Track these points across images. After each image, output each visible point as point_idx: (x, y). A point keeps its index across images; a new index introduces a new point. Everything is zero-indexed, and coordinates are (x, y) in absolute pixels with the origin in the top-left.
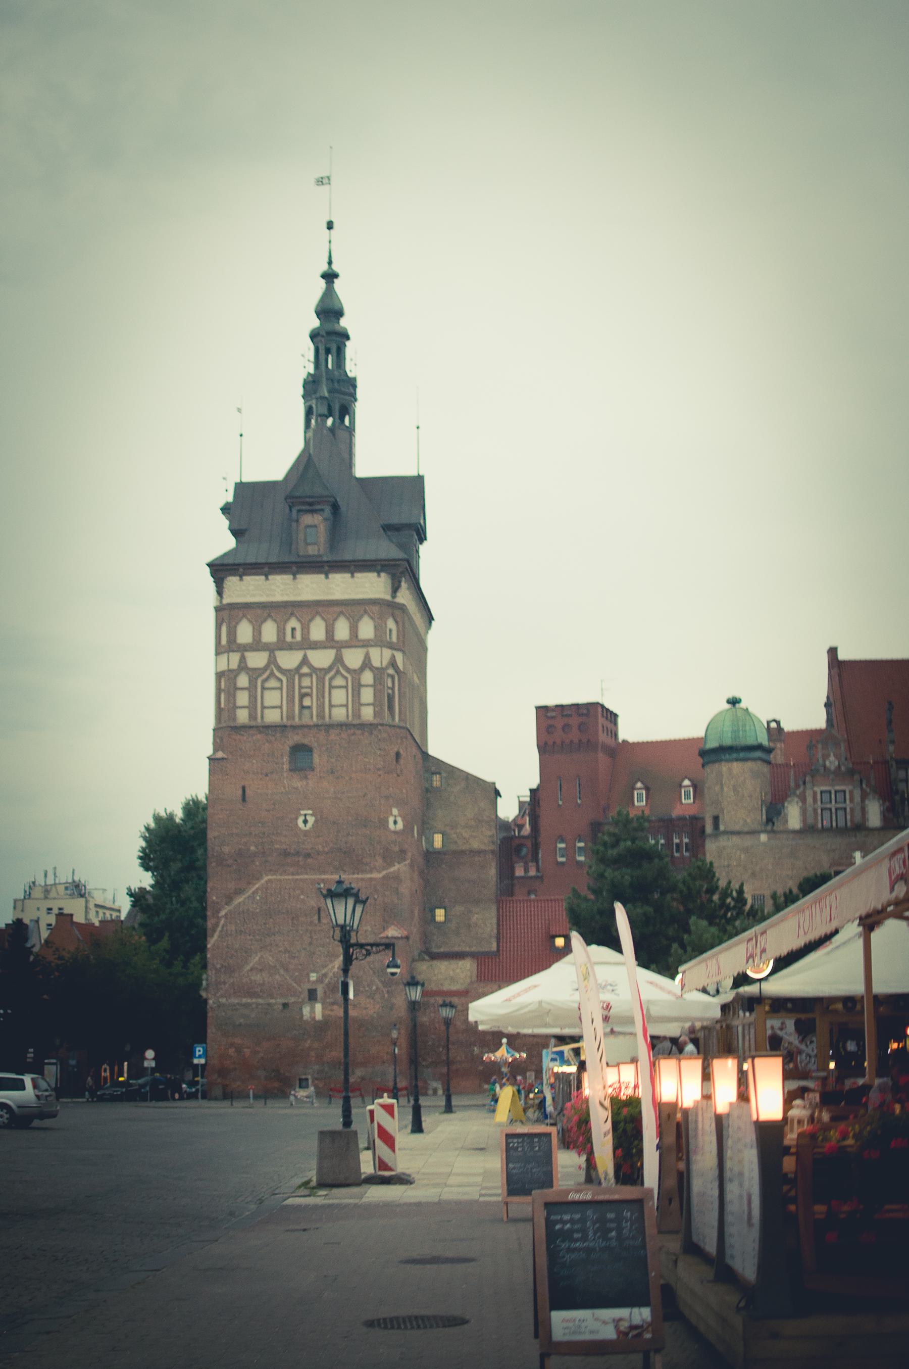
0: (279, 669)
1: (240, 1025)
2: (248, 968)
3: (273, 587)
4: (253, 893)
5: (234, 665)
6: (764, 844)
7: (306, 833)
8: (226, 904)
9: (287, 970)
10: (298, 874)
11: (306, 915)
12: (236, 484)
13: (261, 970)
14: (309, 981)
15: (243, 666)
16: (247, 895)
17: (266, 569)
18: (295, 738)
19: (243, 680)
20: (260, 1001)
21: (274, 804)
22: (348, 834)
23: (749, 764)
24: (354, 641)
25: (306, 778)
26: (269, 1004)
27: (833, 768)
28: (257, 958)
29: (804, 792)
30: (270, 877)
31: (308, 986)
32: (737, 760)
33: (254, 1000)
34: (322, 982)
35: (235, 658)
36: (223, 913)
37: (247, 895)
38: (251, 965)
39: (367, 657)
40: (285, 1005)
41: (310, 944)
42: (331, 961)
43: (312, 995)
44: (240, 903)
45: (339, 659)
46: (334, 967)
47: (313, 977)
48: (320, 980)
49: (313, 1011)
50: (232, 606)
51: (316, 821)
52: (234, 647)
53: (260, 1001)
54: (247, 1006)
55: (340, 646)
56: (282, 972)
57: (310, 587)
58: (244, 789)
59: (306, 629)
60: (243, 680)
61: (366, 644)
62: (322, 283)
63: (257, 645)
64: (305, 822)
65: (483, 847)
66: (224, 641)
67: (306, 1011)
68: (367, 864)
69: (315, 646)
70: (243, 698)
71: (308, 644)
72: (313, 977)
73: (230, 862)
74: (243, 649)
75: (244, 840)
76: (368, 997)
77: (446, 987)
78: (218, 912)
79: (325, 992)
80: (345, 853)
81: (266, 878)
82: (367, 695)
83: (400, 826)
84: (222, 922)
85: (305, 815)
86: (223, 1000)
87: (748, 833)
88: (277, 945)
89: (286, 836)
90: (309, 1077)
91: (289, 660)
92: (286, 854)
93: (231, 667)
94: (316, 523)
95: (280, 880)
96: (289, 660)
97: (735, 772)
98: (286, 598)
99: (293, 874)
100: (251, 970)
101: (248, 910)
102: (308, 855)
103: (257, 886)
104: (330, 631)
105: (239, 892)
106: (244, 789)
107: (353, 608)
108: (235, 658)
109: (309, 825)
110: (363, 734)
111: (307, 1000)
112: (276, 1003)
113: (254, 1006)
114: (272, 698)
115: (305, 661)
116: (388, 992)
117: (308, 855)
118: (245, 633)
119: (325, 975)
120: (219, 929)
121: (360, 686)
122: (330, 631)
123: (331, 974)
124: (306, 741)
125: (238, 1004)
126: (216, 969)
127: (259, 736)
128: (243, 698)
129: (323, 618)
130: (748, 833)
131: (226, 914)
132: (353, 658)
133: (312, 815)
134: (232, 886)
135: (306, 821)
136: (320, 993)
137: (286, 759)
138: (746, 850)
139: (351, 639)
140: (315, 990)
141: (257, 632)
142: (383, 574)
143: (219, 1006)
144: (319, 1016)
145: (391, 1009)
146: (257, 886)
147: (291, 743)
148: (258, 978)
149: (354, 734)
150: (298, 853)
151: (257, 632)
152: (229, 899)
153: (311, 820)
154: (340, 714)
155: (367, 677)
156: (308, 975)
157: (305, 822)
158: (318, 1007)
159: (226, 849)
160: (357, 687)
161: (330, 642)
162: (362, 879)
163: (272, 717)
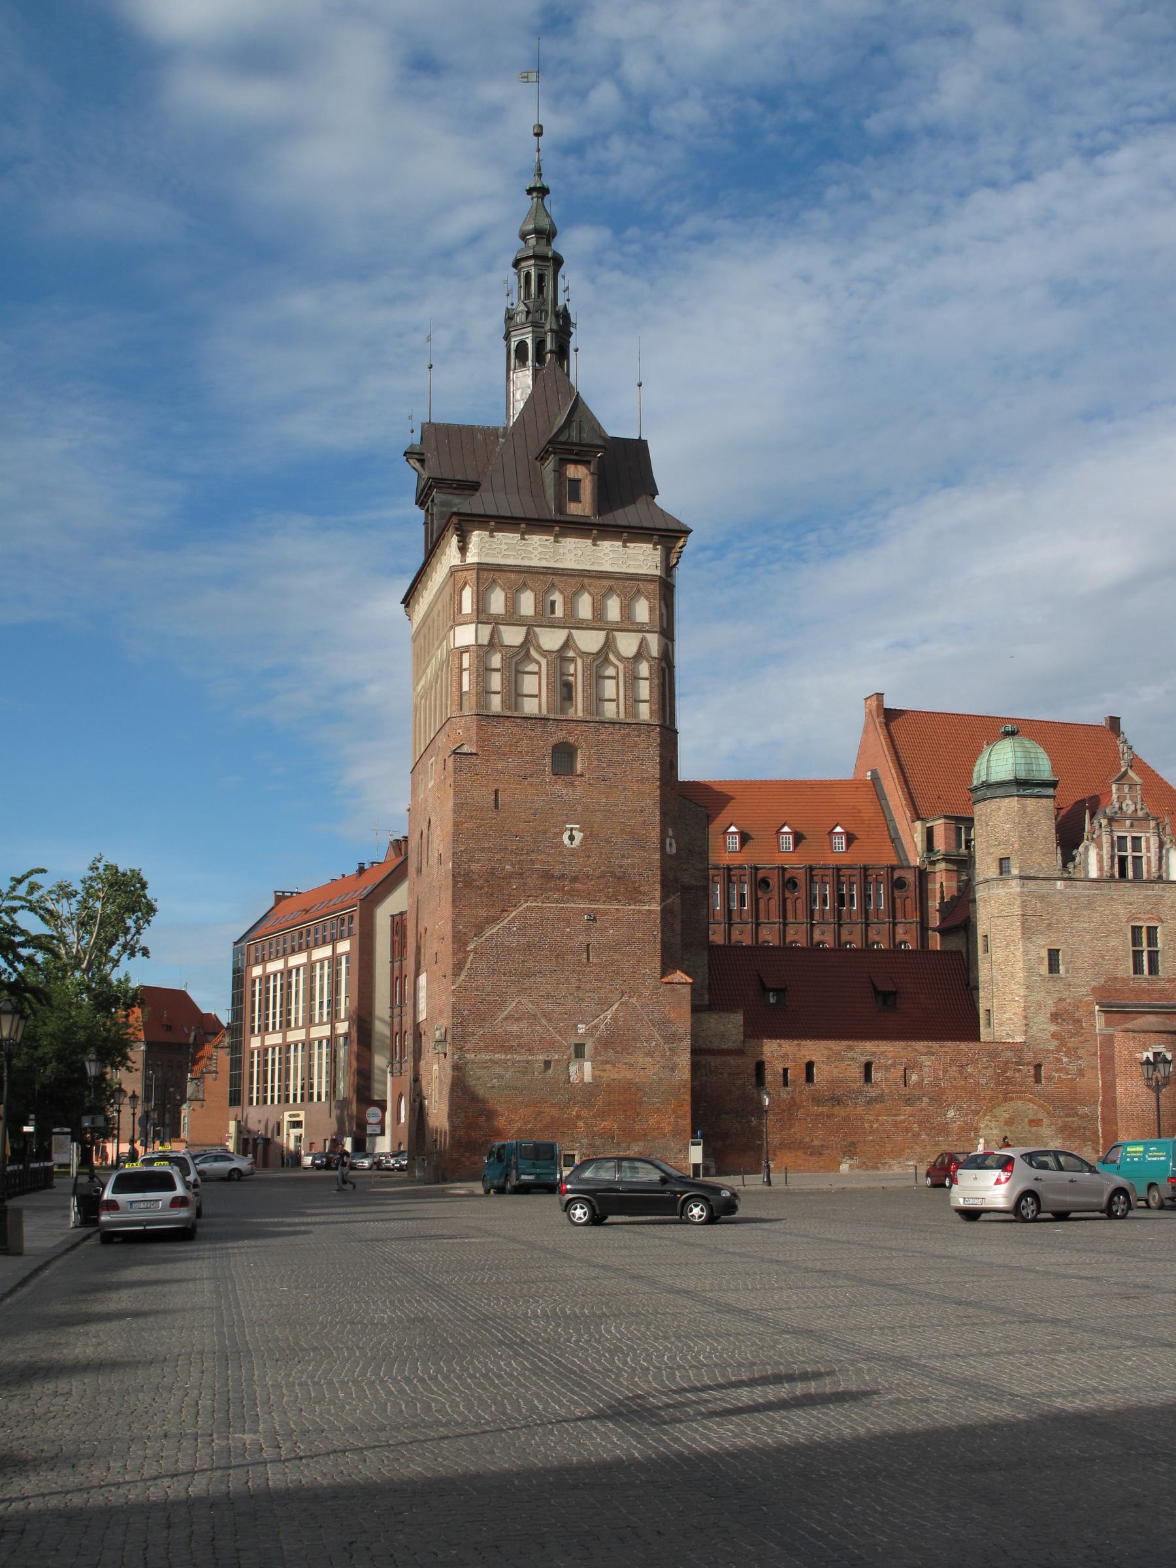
0: (539, 648)
1: (493, 1087)
2: (503, 1016)
3: (530, 549)
4: (510, 923)
5: (484, 640)
6: (1060, 892)
7: (573, 852)
8: (475, 935)
9: (550, 1021)
10: (563, 902)
11: (573, 953)
12: (423, 425)
13: (518, 1019)
14: (577, 1034)
15: (494, 643)
17: (523, 526)
18: (558, 736)
19: (496, 661)
20: (518, 1058)
21: (535, 814)
22: (623, 856)
23: (1044, 801)
24: (628, 624)
25: (572, 784)
27: (1130, 812)
29: (1100, 836)
30: (529, 904)
31: (575, 1040)
32: (1031, 796)
34: (592, 1035)
35: (486, 631)
36: (471, 947)
39: (643, 644)
41: (578, 988)
43: (579, 1051)
45: (609, 645)
47: (582, 1028)
48: (589, 1033)
49: (581, 1068)
50: (481, 567)
51: (584, 838)
52: (483, 617)
53: (518, 1058)
55: (611, 630)
56: (544, 1022)
57: (575, 553)
58: (496, 792)
59: (571, 604)
60: (496, 661)
61: (640, 629)
62: (528, 202)
63: (512, 617)
64: (572, 838)
65: (694, 883)
66: (467, 607)
67: (573, 1069)
68: (645, 893)
69: (581, 625)
70: (496, 682)
71: (572, 622)
72: (582, 1028)
73: (480, 883)
74: (496, 622)
75: (497, 857)
76: (647, 1055)
77: (716, 1044)
78: (466, 944)
79: (596, 1048)
80: (619, 878)
81: (525, 905)
82: (644, 689)
83: (674, 851)
84: (471, 958)
85: (571, 829)
87: (1043, 879)
89: (549, 854)
90: (576, 1152)
91: (551, 639)
92: (548, 876)
93: (480, 642)
94: (580, 476)
95: (542, 908)
96: (551, 639)
97: (1028, 809)
98: (545, 564)
99: (557, 902)
100: (506, 1018)
101: (502, 943)
102: (575, 879)
103: (513, 914)
104: (599, 610)
106: (496, 792)
107: (626, 584)
108: (486, 631)
109: (577, 842)
110: (639, 736)
113: (509, 1063)
114: (530, 684)
115: (568, 644)
116: (670, 1049)
117: (575, 879)
118: (497, 602)
119: (596, 1027)
120: (468, 965)
121: (637, 678)
122: (599, 610)
123: (602, 1026)
124: (572, 740)
127: (515, 730)
128: (496, 682)
129: (590, 594)
130: (1043, 879)
131: (475, 949)
132: (627, 644)
133: (580, 830)
134: (483, 912)
135: (573, 838)
136: (588, 1050)
137: (548, 760)
138: (1042, 898)
139: (622, 621)
141: (512, 603)
142: (659, 547)
144: (588, 1078)
145: (673, 1070)
146: (513, 914)
147: (554, 740)
148: (514, 1028)
149: (629, 735)
150: (562, 877)
151: (512, 603)
152: (479, 929)
153: (579, 836)
154: (610, 711)
155: (644, 669)
157: (572, 838)
158: (588, 1066)
159: (475, 867)
160: (633, 679)
161: (598, 621)
162: (640, 911)
163: (530, 707)
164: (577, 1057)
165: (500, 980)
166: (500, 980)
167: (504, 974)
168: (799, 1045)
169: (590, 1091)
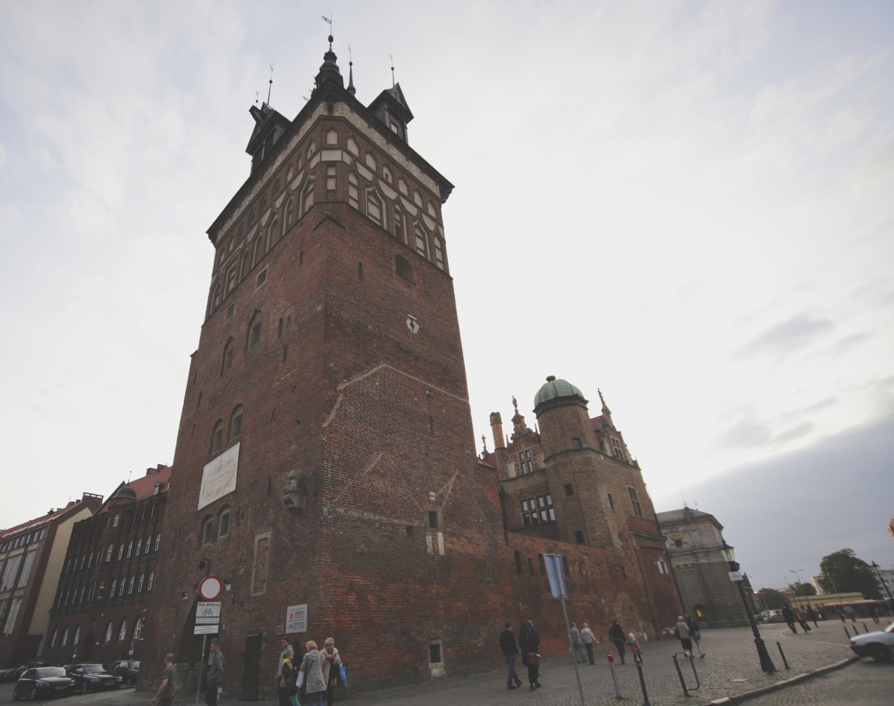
2: (369, 468)
8: (345, 377)
9: (408, 482)
10: (410, 373)
13: (383, 476)
14: (429, 501)
16: (366, 375)
26: (393, 525)
28: (379, 458)
31: (429, 508)
33: (377, 517)
36: (341, 387)
37: (366, 375)
38: (372, 466)
40: (409, 529)
41: (427, 454)
42: (446, 481)
44: (358, 381)
46: (448, 488)
48: (438, 502)
49: (435, 539)
54: (368, 523)
73: (349, 330)
78: (337, 383)
79: (444, 519)
84: (340, 398)
86: (341, 510)
88: (397, 447)
95: (395, 372)
100: (374, 472)
101: (367, 393)
105: (360, 369)
111: (428, 525)
112: (400, 526)
117: (417, 358)
120: (337, 406)
125: (359, 519)
126: (333, 461)
140: (436, 513)
143: (336, 520)
144: (442, 551)
146: (375, 369)
148: (380, 484)
153: (417, 327)
156: (427, 492)
157: (412, 325)
158: (440, 535)
164: (431, 526)
165: (366, 430)
166: (366, 430)
167: (370, 425)
168: (532, 540)
169: (448, 561)
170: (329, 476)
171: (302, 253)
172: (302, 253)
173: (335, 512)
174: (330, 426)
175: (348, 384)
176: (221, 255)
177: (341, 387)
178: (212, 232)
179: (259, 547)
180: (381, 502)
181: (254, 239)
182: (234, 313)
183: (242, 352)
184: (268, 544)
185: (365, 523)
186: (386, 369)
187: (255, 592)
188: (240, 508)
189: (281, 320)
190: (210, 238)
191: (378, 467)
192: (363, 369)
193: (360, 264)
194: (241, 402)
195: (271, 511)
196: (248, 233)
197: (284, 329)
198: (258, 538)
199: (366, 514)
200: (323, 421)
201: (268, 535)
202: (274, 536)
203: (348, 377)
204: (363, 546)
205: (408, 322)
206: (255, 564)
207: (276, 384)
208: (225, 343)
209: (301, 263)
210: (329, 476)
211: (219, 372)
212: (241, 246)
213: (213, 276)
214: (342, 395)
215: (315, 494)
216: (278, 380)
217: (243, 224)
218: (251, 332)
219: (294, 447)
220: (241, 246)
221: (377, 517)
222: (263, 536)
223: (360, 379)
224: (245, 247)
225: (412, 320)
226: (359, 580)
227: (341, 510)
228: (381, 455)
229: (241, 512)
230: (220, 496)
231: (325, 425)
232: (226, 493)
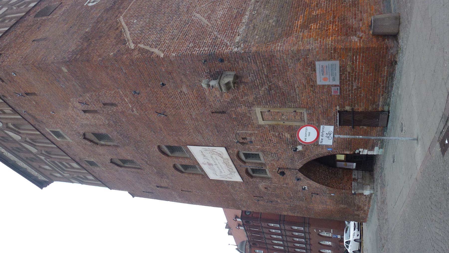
2: (206, 21)
8: (125, 44)
16: (127, 30)
28: (198, 15)
33: (248, 13)
36: (132, 46)
37: (127, 30)
38: (203, 19)
44: (130, 34)
73: (86, 44)
84: (142, 46)
86: (238, 39)
95: (129, 10)
100: (209, 18)
101: (141, 27)
120: (147, 48)
125: (247, 25)
143: (245, 42)
146: (123, 24)
148: (220, 13)
165: (172, 26)
166: (172, 26)
170: (206, 49)
171: (27, 94)
172: (27, 94)
173: (238, 42)
174: (163, 52)
175: (131, 41)
176: (56, 177)
177: (132, 46)
178: (41, 184)
179: (268, 120)
180: (235, 11)
181: (34, 146)
182: (92, 160)
183: (119, 150)
184: (264, 110)
185: (251, 21)
186: (125, 17)
187: (304, 121)
188: (238, 142)
189: (85, 111)
190: (46, 186)
191: (206, 15)
192: (121, 32)
193: (34, 41)
194: (156, 147)
195: (239, 109)
196: (31, 152)
197: (90, 108)
198: (261, 122)
199: (244, 21)
200: (158, 57)
201: (258, 110)
202: (259, 104)
203: (124, 42)
204: (271, 21)
205: (90, 4)
206: (282, 123)
207: (135, 112)
208: (117, 167)
209: (34, 94)
210: (206, 49)
211: (139, 171)
212: (43, 158)
213: (73, 182)
214: (139, 45)
215: (222, 61)
216: (133, 111)
217: (27, 158)
218: (102, 142)
219: (184, 89)
220: (43, 158)
221: (248, 13)
222: (259, 116)
223: (128, 33)
224: (42, 154)
225: (89, 2)
226: (300, 21)
227: (238, 39)
228: (195, 14)
229: (242, 141)
230: (231, 163)
231: (162, 55)
232: (228, 157)
